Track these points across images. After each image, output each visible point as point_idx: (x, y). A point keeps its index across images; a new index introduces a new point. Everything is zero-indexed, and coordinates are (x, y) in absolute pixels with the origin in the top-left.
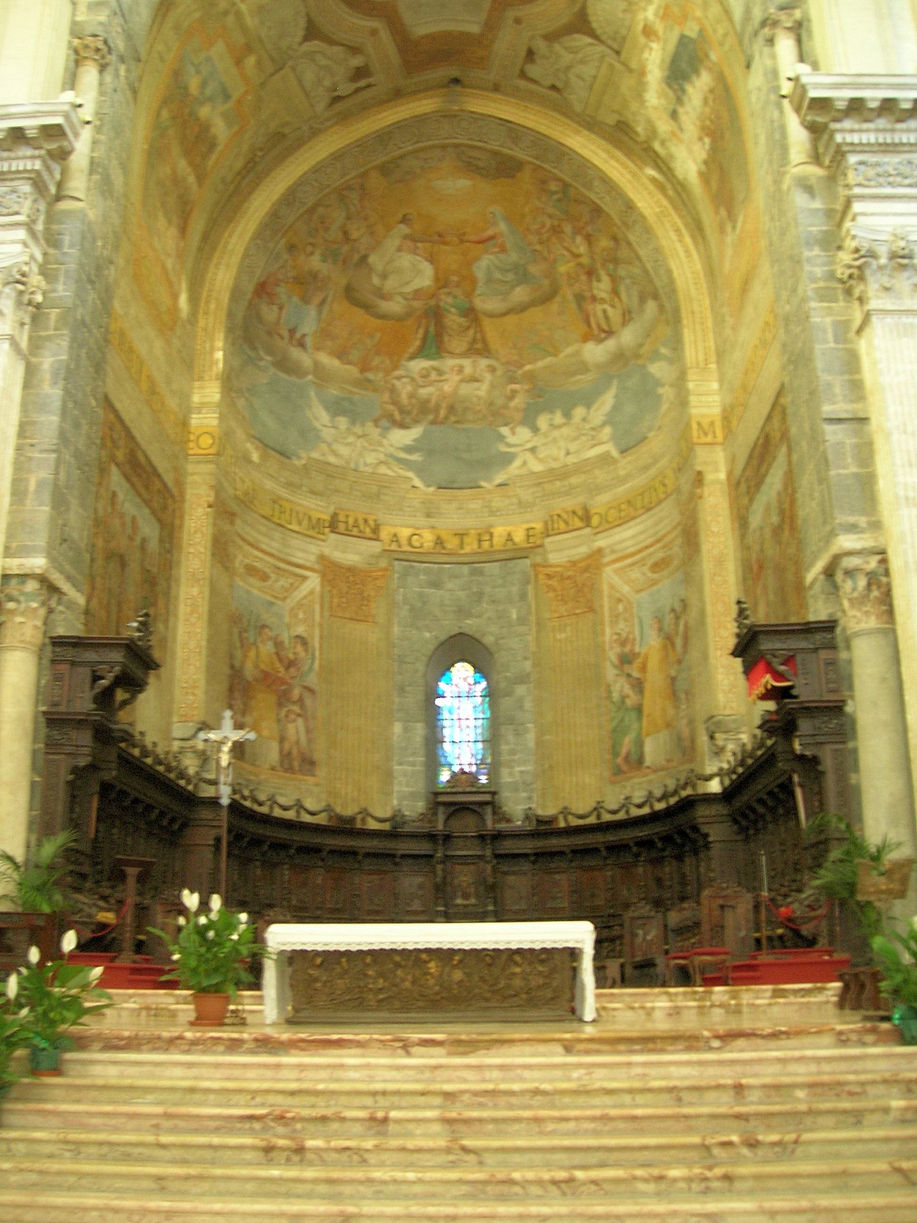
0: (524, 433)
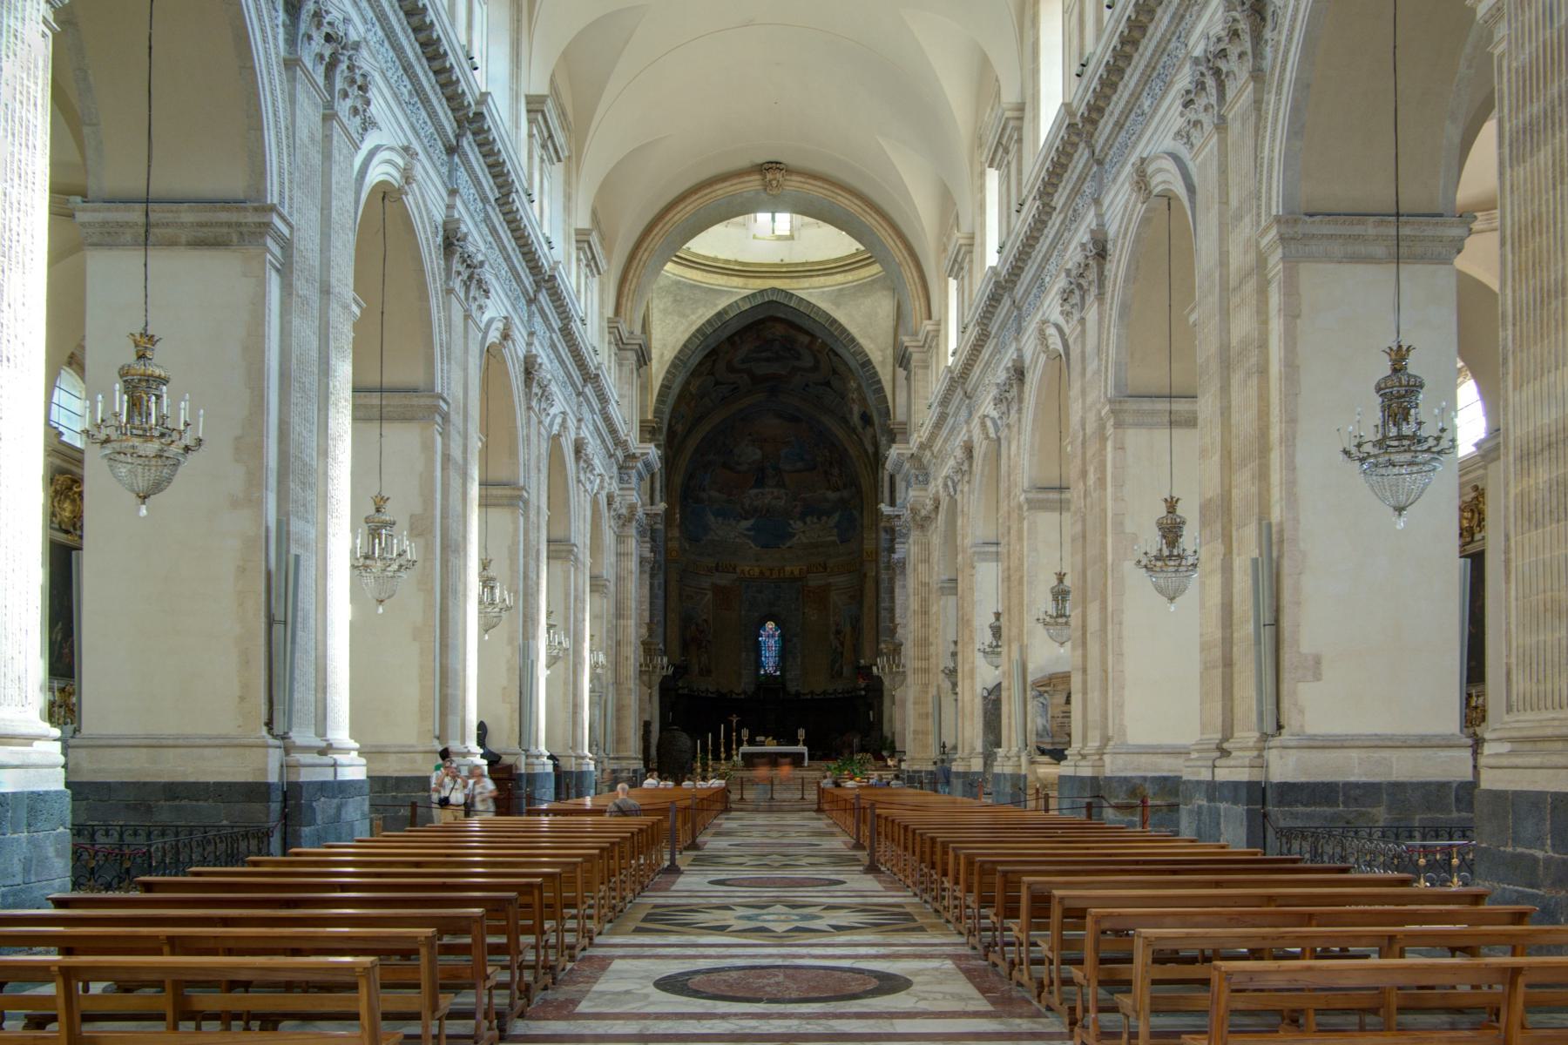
0: (799, 524)
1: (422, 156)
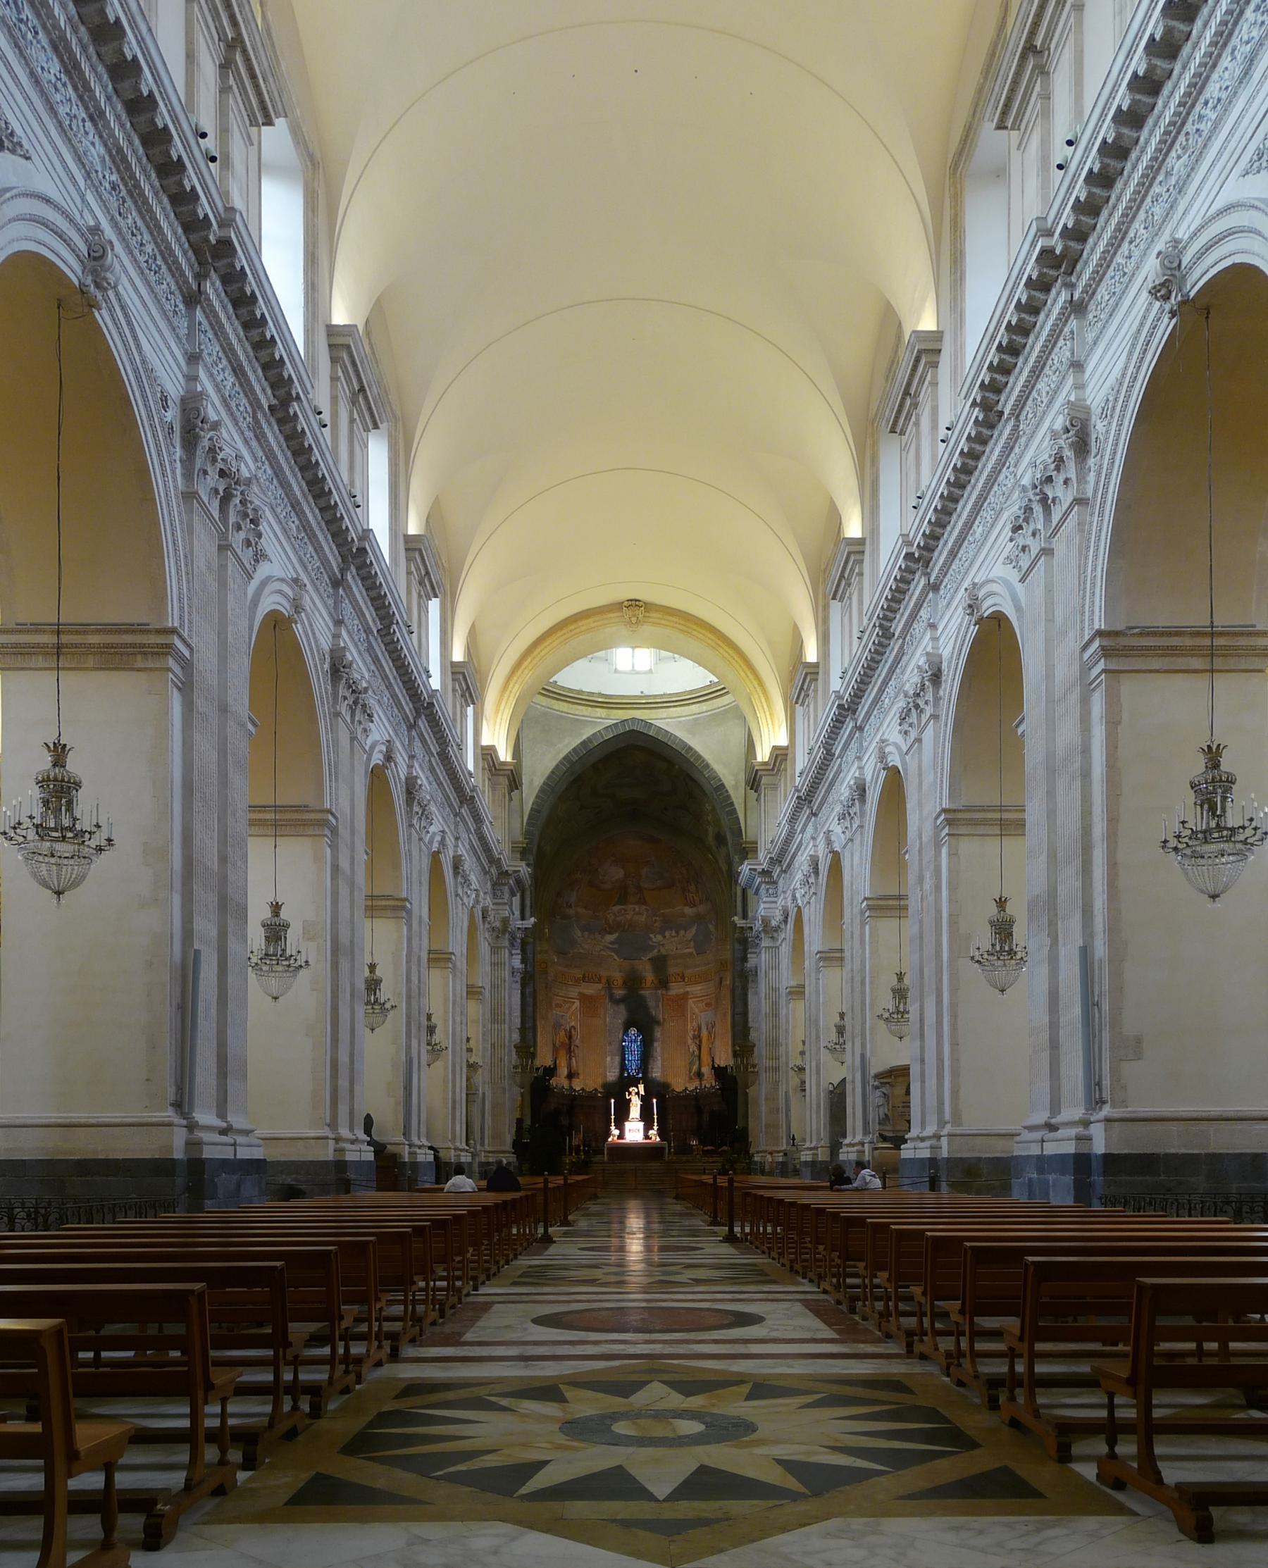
0: (659, 937)
1: (309, 587)
